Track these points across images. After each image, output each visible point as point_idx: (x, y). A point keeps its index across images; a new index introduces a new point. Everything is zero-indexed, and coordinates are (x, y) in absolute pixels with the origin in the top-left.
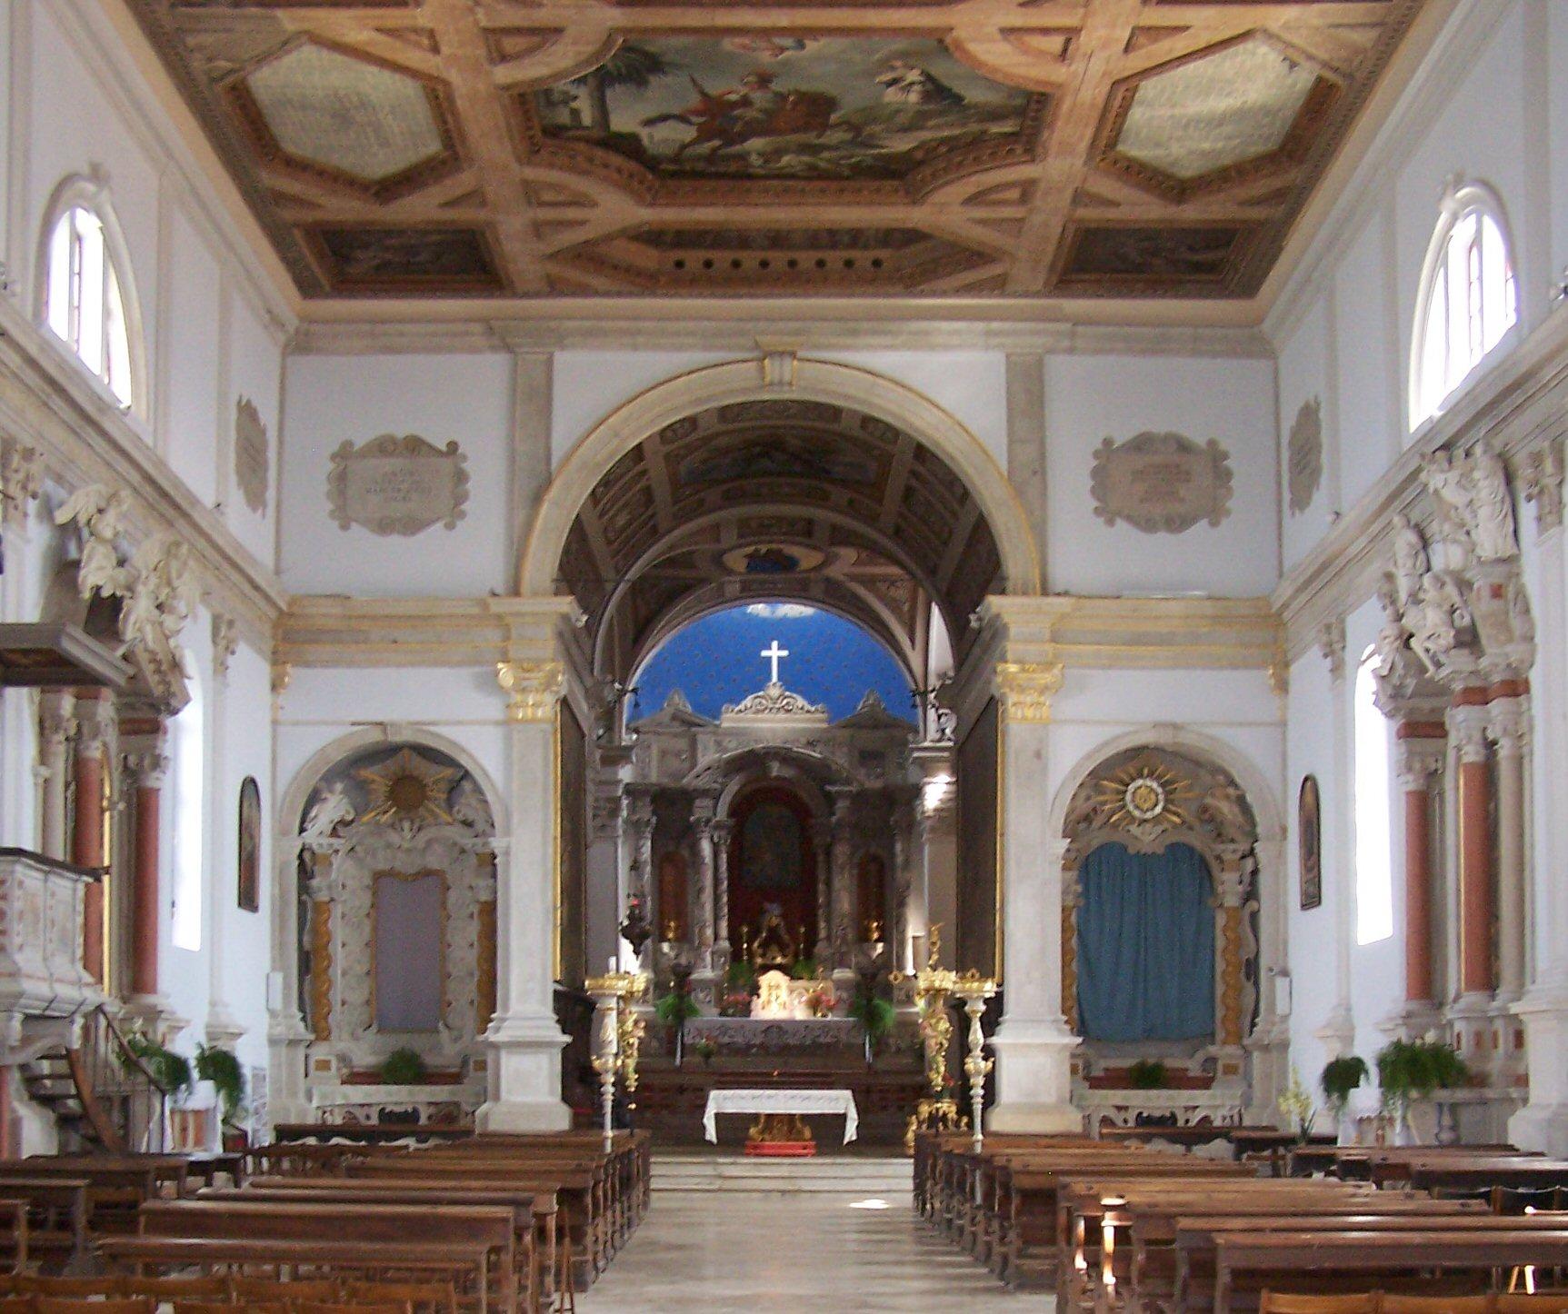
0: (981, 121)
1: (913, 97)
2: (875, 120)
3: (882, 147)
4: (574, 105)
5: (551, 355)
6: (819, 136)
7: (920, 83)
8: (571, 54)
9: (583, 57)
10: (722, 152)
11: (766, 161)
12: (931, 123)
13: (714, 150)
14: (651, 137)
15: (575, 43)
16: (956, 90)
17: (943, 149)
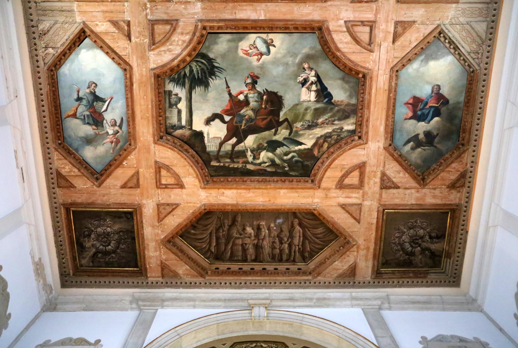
0: (339, 120)
1: (313, 96)
2: (296, 119)
3: (301, 144)
4: (180, 106)
5: (157, 310)
6: (275, 134)
7: (316, 83)
8: (180, 43)
9: (185, 44)
10: (236, 148)
11: (254, 158)
12: (320, 121)
13: (234, 146)
14: (208, 134)
15: (182, 34)
16: (329, 90)
17: (326, 145)
